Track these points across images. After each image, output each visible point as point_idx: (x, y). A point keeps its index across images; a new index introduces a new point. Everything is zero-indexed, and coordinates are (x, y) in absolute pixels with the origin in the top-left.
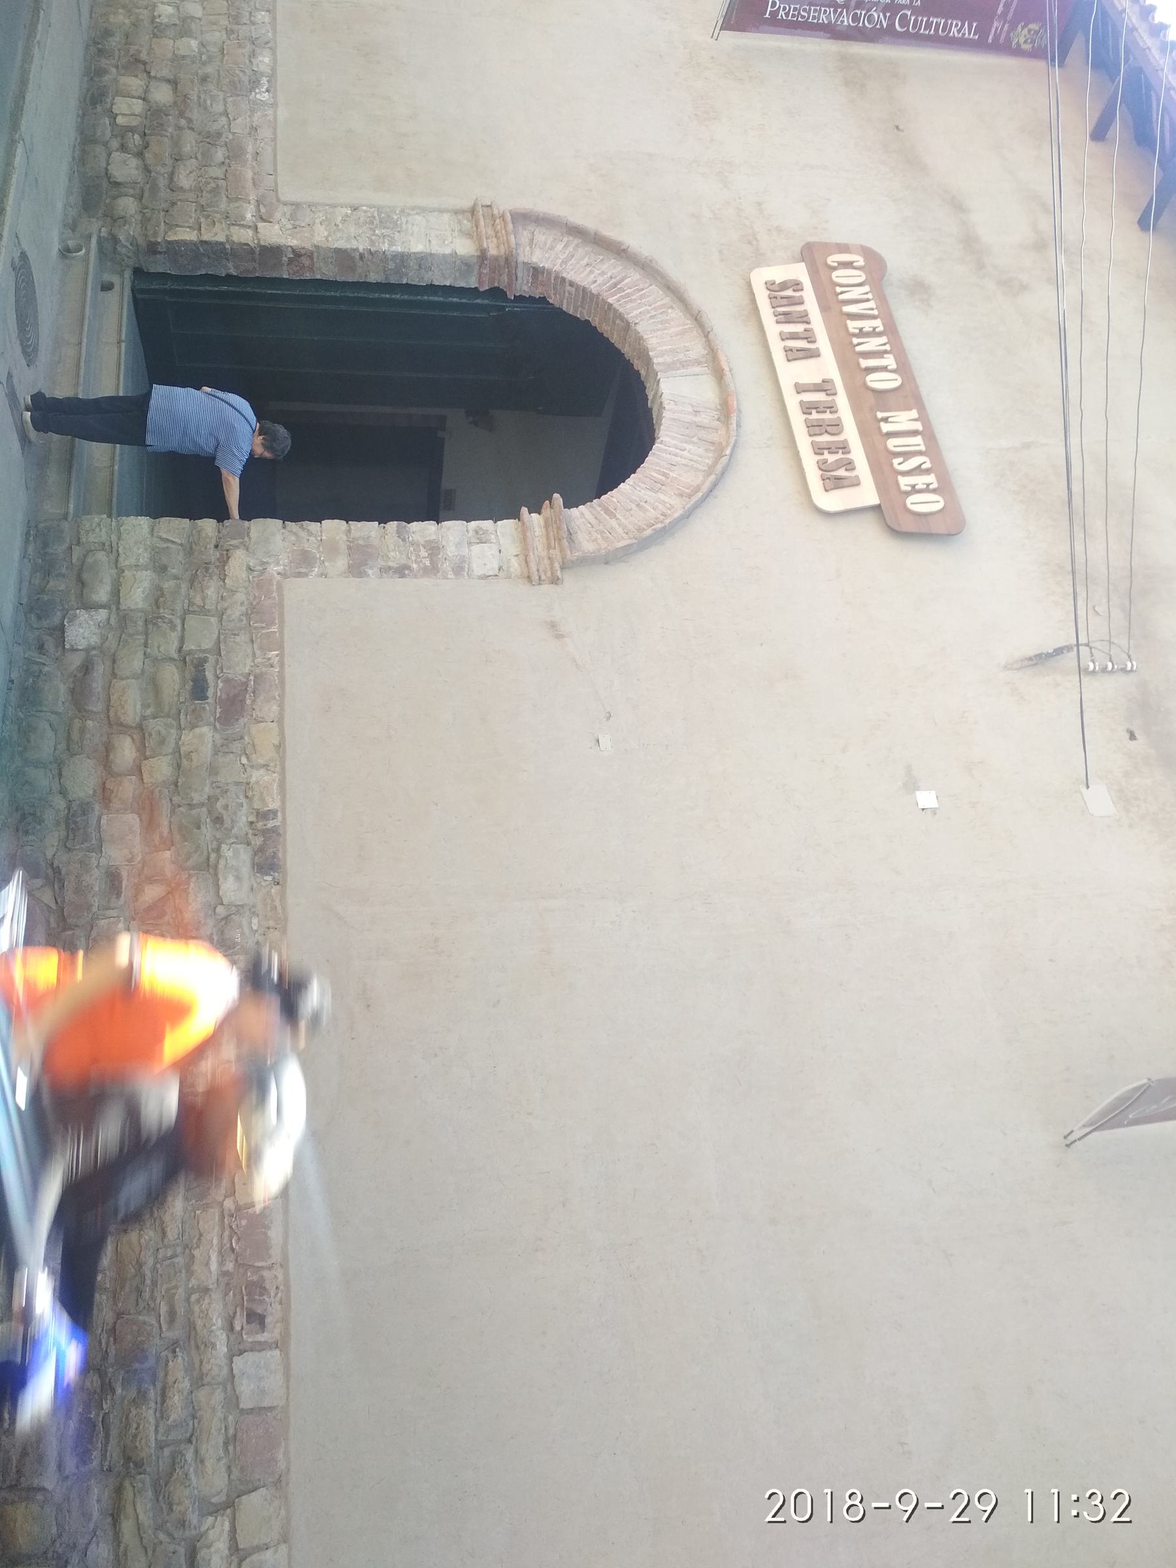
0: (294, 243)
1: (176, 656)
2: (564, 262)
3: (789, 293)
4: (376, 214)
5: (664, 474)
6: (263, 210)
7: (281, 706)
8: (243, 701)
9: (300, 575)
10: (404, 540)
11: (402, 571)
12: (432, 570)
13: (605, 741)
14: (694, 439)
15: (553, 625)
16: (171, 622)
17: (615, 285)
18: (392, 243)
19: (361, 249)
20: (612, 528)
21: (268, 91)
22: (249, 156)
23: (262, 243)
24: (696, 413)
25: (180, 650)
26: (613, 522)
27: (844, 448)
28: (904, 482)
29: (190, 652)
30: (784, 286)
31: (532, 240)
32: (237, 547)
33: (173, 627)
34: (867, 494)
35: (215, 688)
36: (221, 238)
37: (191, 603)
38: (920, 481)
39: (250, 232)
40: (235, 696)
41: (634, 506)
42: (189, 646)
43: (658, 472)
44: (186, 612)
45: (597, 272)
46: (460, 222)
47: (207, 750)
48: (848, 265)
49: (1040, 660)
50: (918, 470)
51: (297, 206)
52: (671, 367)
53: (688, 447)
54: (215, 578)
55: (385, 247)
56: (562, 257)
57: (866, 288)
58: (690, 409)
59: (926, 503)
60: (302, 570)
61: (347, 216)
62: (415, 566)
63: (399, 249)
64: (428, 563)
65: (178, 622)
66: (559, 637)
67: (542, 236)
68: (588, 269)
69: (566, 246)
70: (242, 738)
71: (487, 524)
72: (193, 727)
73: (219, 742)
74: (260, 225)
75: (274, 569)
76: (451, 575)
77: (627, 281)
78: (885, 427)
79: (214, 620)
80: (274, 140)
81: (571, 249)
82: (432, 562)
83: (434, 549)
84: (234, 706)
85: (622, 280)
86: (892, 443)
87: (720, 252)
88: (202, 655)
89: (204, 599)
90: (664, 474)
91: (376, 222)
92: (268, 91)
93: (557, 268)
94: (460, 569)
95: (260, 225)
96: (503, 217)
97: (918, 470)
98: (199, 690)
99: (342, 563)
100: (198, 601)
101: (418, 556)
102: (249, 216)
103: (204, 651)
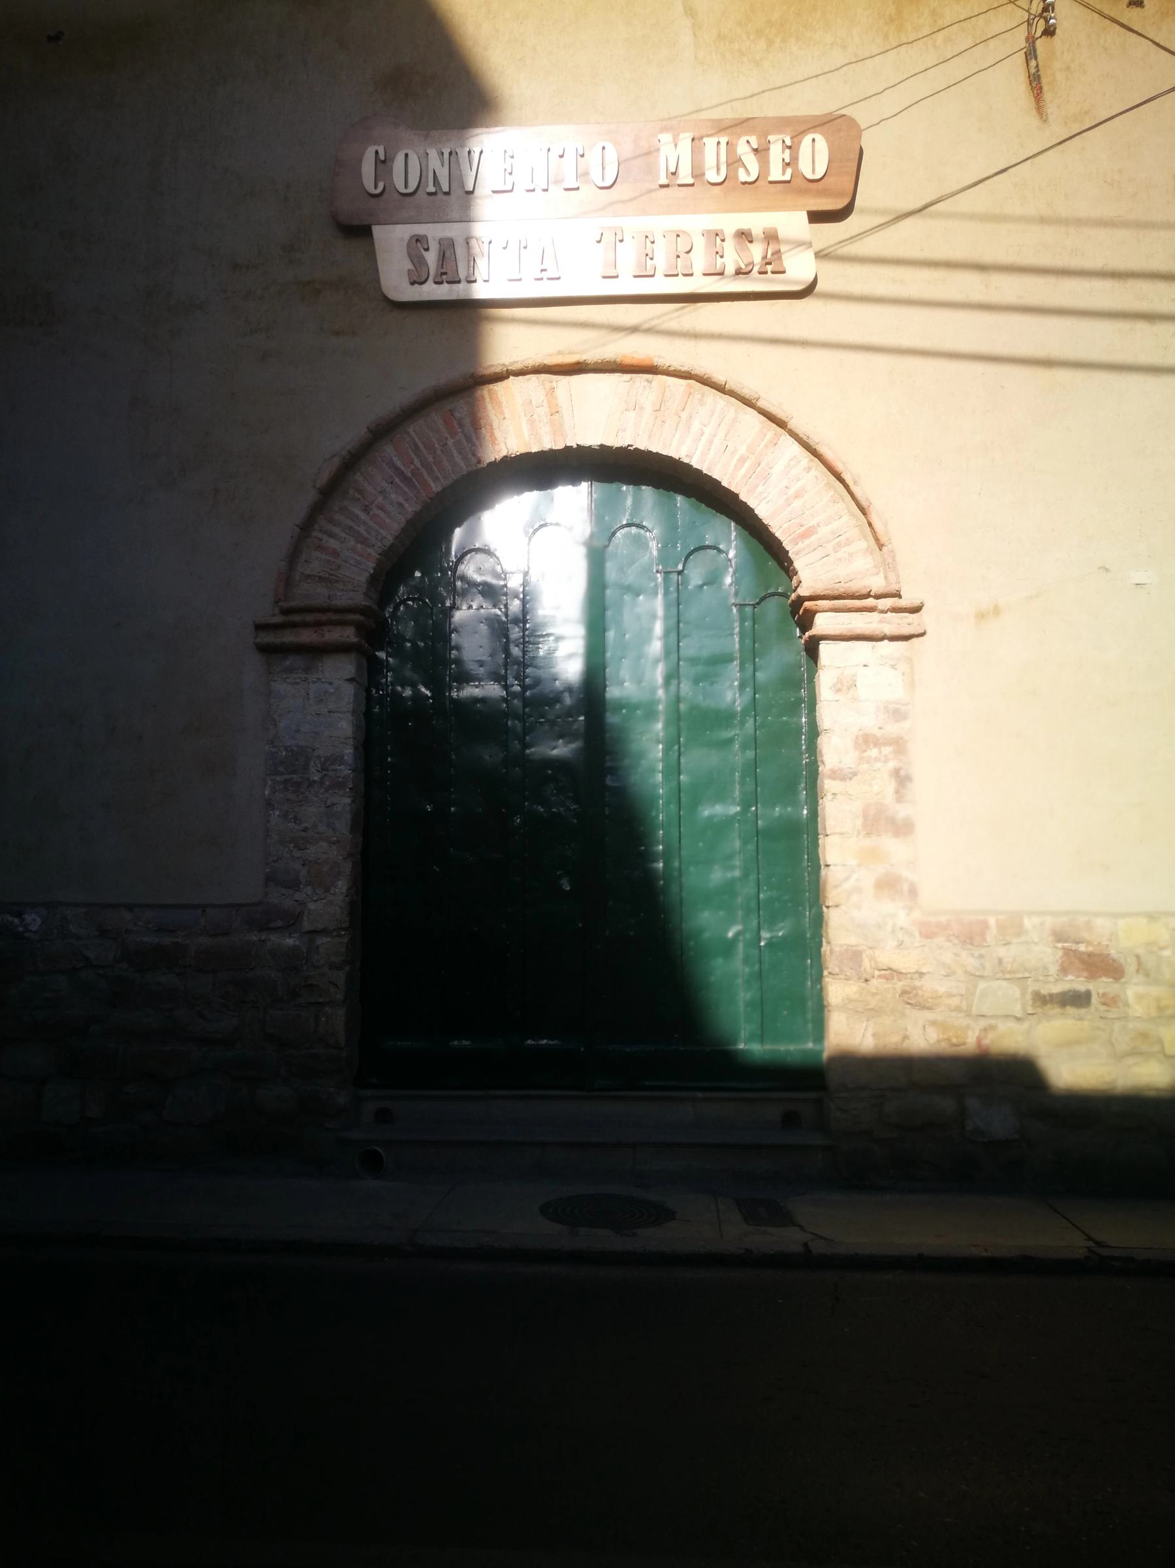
0: (342, 886)
1: (1026, 1025)
2: (364, 541)
3: (431, 258)
4: (278, 778)
5: (743, 460)
6: (279, 923)
7: (1097, 914)
8: (1090, 955)
9: (913, 892)
10: (855, 774)
11: (902, 779)
12: (899, 745)
13: (1138, 577)
14: (684, 415)
15: (981, 616)
16: (985, 1030)
17: (405, 479)
18: (339, 759)
19: (348, 801)
20: (833, 533)
21: (19, 915)
22: (167, 940)
23: (346, 925)
24: (637, 407)
25: (1018, 1019)
26: (823, 531)
27: (716, 235)
28: (776, 174)
29: (1024, 1008)
30: (418, 261)
31: (321, 579)
32: (872, 959)
33: (992, 1028)
34: (792, 222)
35: (1076, 983)
36: (340, 977)
37: (958, 1009)
38: (777, 154)
39: (322, 940)
40: (1083, 962)
41: (797, 504)
42: (1017, 1010)
43: (738, 467)
44: (968, 1014)
45: (380, 499)
46: (289, 670)
47: (1155, 991)
48: (383, 164)
49: (1035, 82)
50: (761, 152)
51: (270, 879)
52: (557, 429)
53: (696, 425)
54: (917, 983)
55: (345, 771)
56: (352, 542)
57: (433, 153)
58: (632, 415)
59: (815, 156)
60: (906, 888)
61: (285, 816)
62: (892, 764)
63: (348, 752)
64: (888, 750)
65: (983, 1023)
66: (997, 611)
67: (314, 563)
68: (375, 511)
69: (331, 535)
70: (1138, 957)
71: (825, 680)
72: (1127, 1004)
73: (1140, 978)
74: (307, 925)
75: (903, 919)
76: (906, 725)
77: (398, 463)
78: (685, 176)
79: (982, 985)
80: (130, 907)
81: (336, 530)
82: (884, 744)
83: (866, 741)
84: (1100, 965)
85: (397, 469)
86: (712, 176)
87: (337, 333)
88: (1029, 997)
89: (950, 995)
90: (743, 460)
91: (296, 778)
92: (19, 915)
93: (374, 553)
94: (897, 714)
95: (307, 925)
96: (285, 612)
97: (761, 152)
98: (1079, 999)
99: (890, 844)
100: (955, 1001)
101: (877, 760)
102: (290, 942)
103: (1023, 994)
